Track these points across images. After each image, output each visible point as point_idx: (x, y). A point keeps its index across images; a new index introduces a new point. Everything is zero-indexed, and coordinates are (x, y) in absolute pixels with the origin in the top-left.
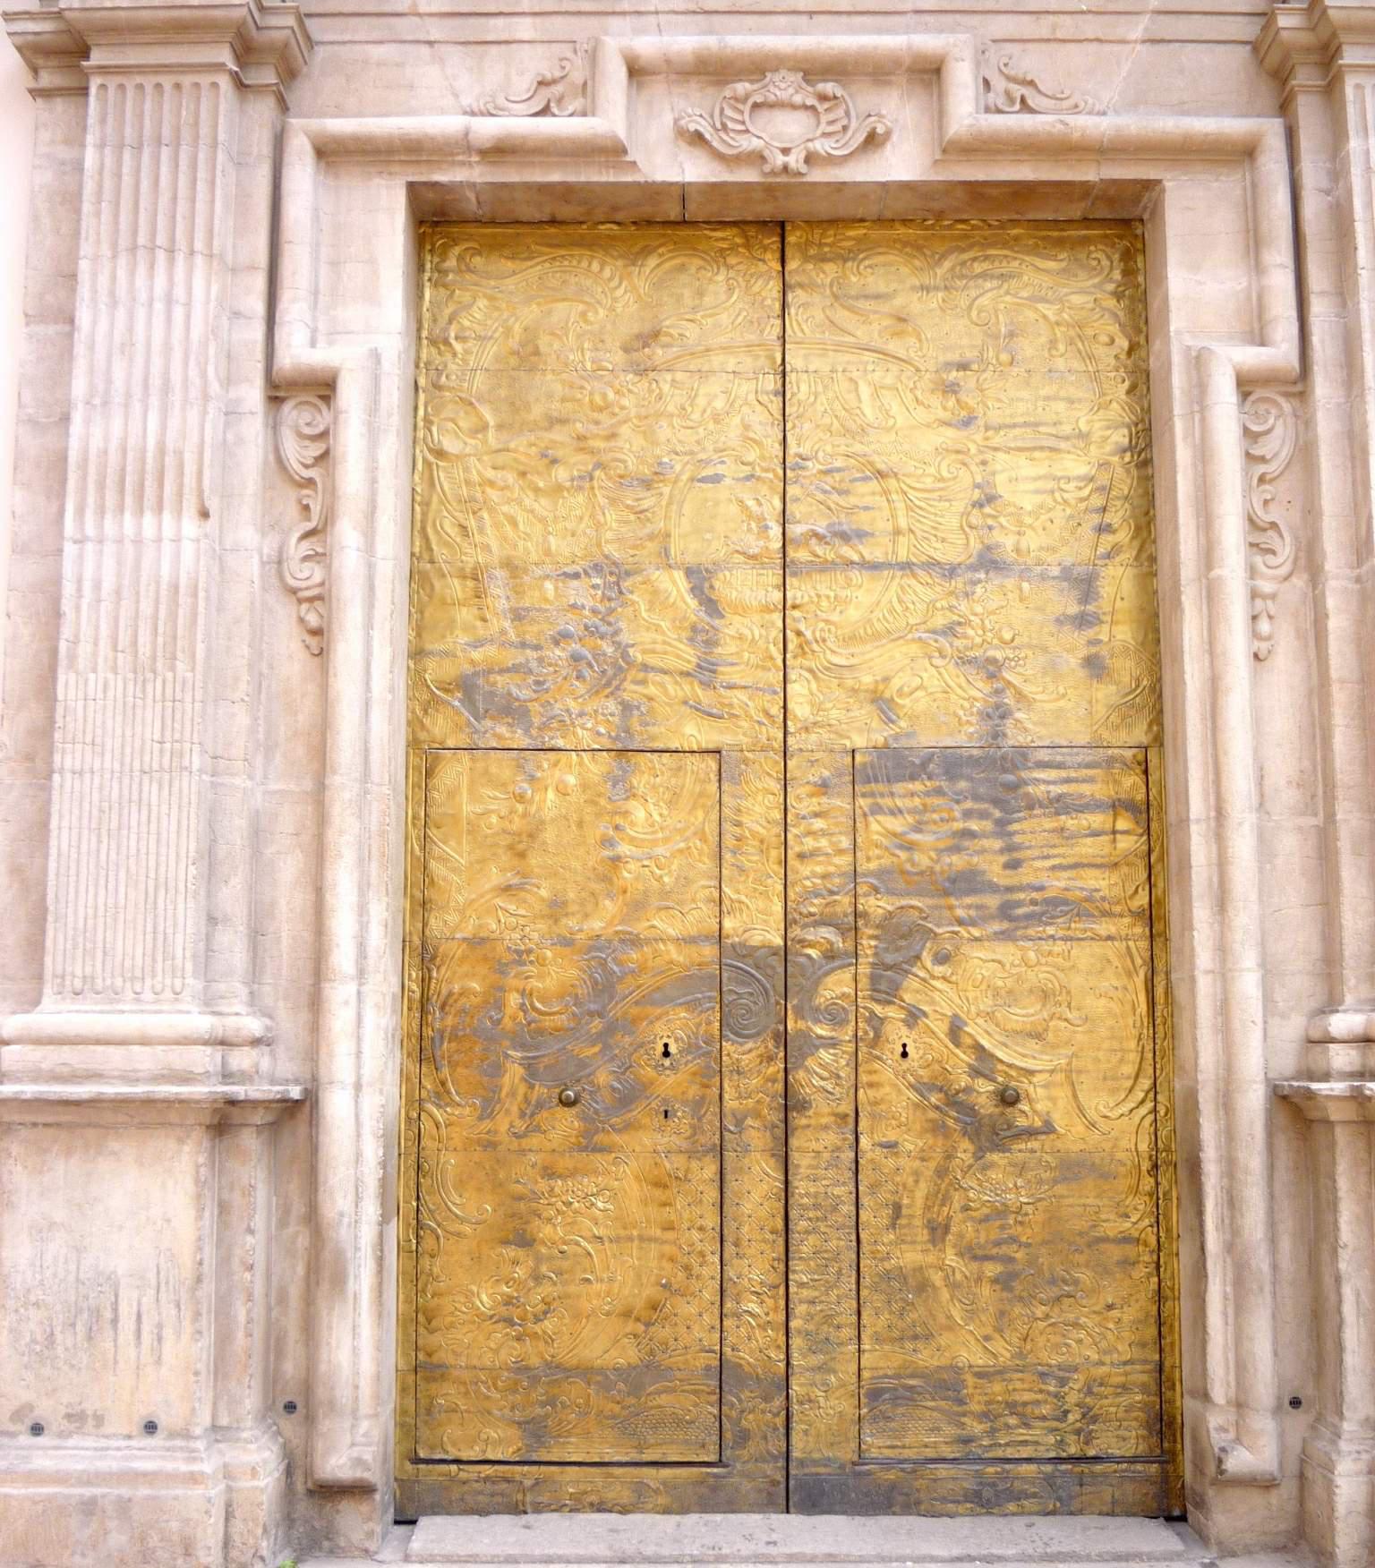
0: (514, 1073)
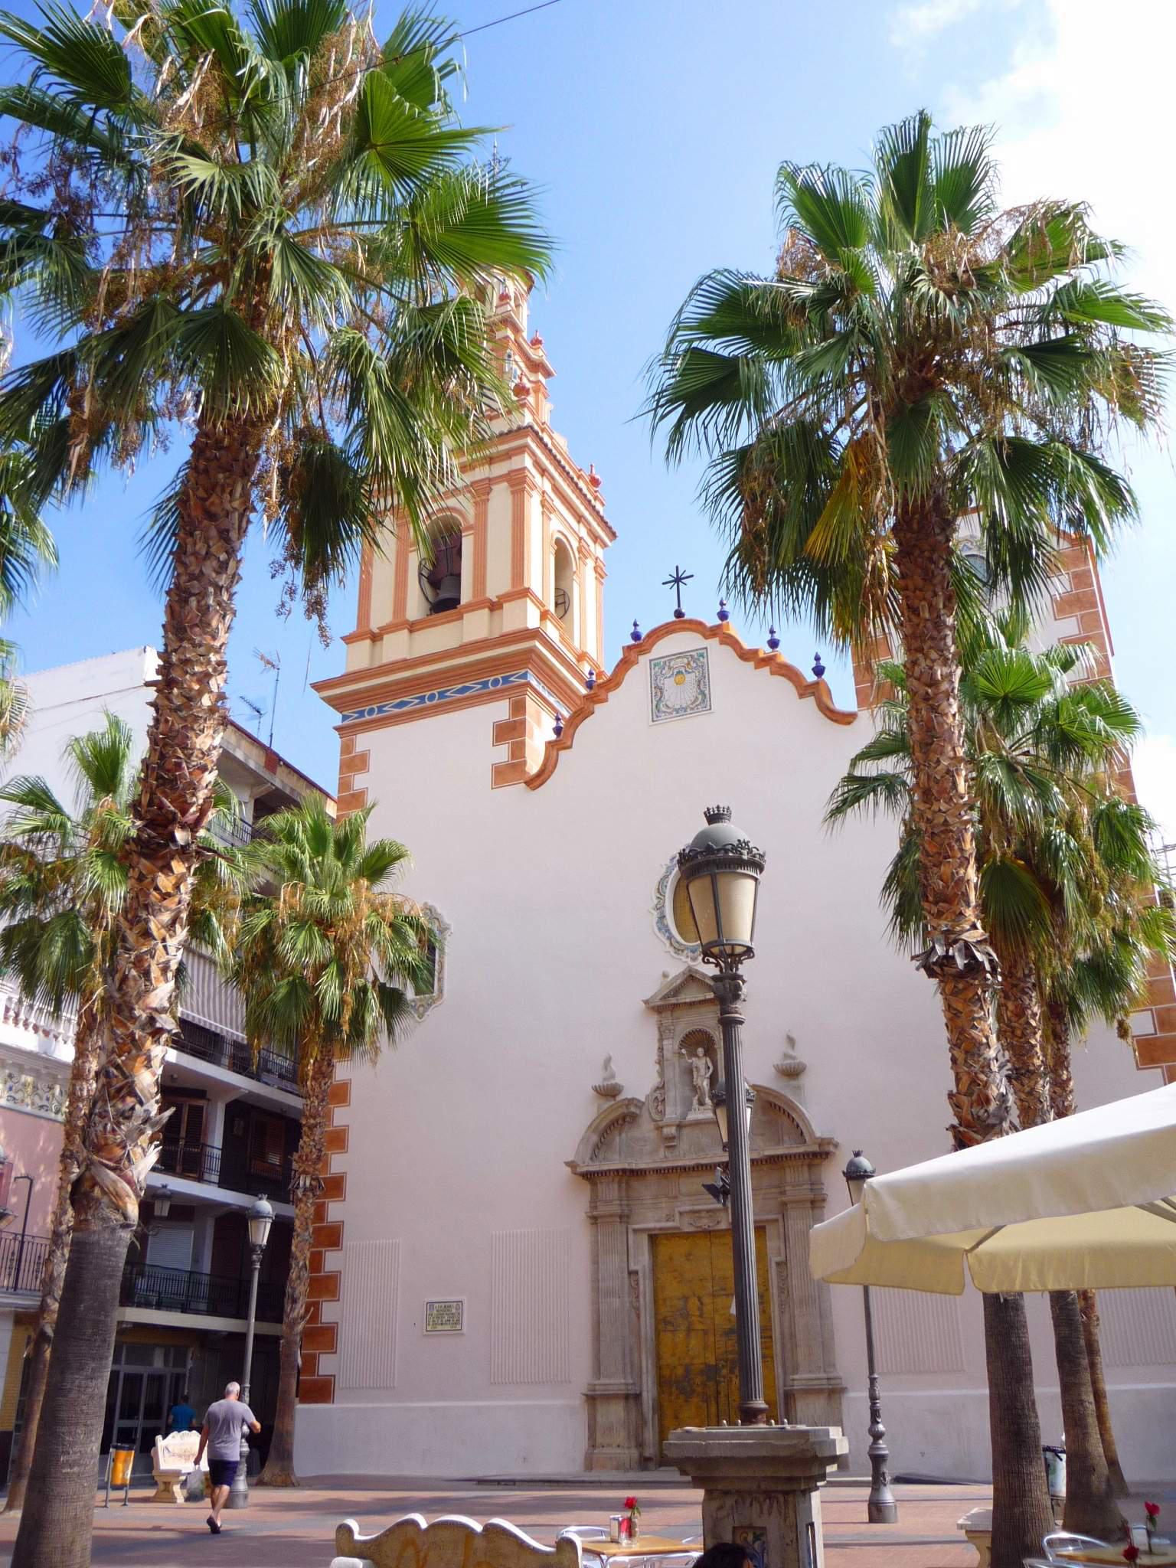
0: (674, 1389)
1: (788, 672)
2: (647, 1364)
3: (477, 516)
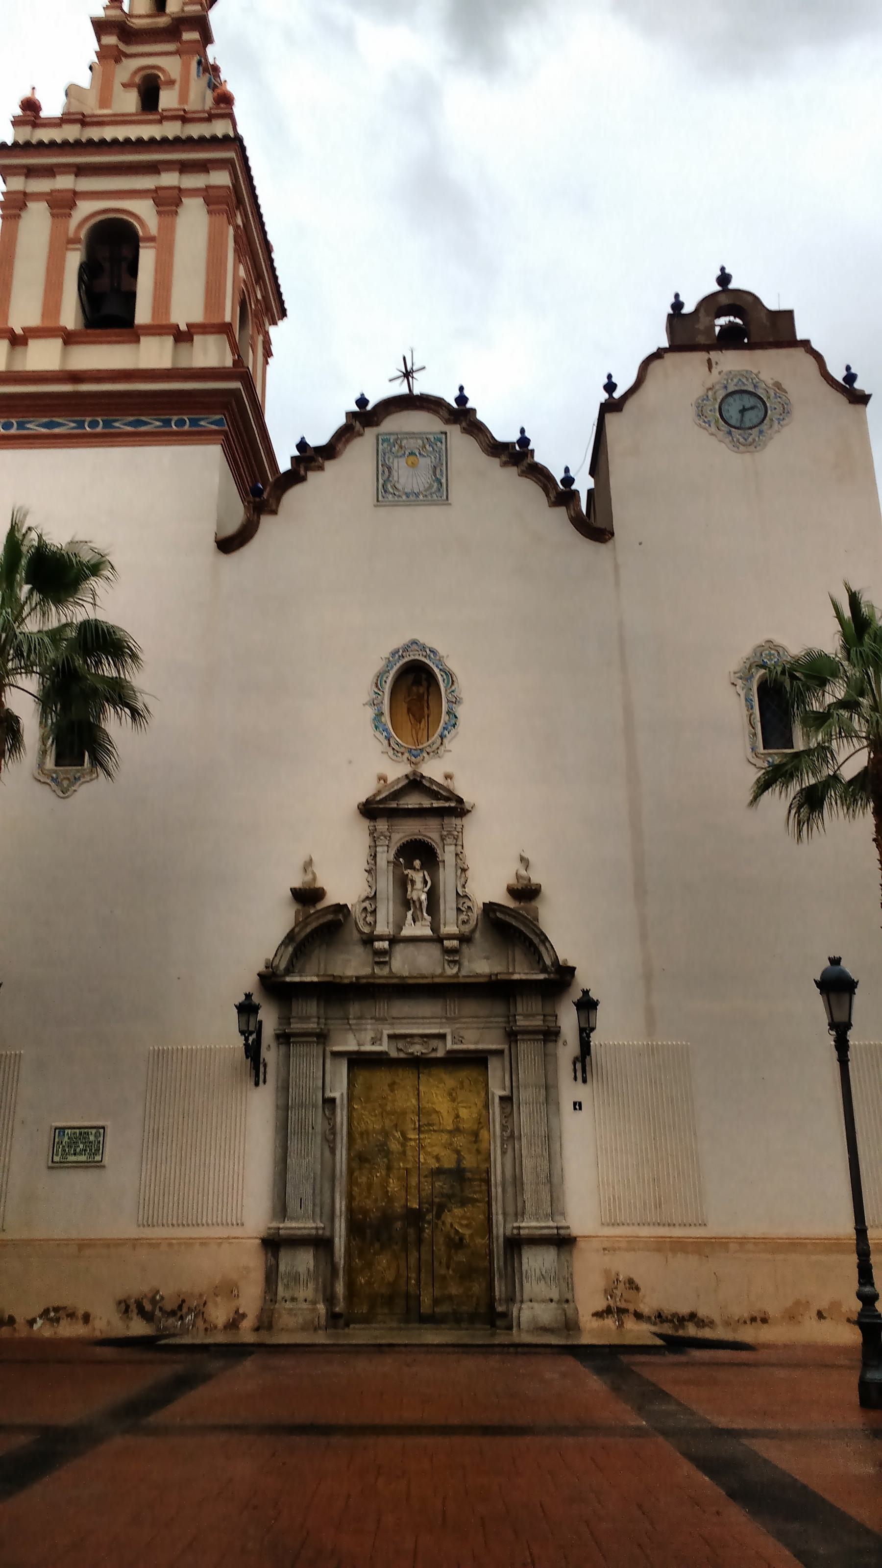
1: (539, 474)
2: (340, 1205)
3: (160, 228)
